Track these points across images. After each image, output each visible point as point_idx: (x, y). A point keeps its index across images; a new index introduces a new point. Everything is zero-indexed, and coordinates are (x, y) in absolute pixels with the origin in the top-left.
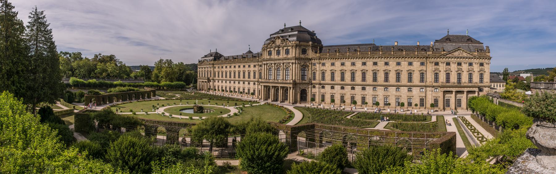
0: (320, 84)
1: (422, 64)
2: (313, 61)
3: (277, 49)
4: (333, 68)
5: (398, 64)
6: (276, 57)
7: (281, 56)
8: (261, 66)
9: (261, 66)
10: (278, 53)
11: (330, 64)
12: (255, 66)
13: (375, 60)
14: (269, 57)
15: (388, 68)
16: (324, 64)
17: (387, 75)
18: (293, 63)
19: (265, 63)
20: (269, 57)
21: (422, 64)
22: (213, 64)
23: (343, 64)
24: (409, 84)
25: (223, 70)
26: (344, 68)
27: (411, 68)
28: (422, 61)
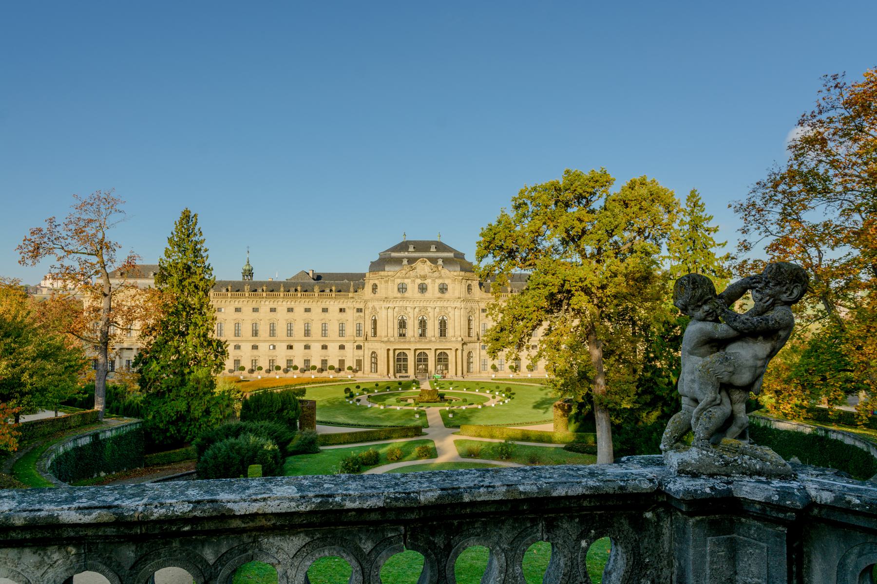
3: (419, 281)
9: (359, 310)
10: (423, 289)
20: (399, 295)
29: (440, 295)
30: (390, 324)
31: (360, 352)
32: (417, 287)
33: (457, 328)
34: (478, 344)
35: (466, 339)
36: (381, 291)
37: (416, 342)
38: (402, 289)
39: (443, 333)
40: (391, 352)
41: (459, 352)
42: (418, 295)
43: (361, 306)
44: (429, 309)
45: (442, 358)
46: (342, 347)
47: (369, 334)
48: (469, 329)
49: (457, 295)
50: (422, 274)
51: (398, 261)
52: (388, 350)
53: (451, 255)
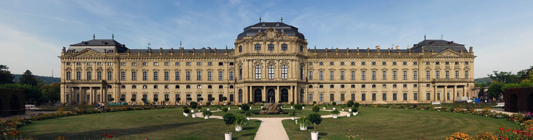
0: (319, 83)
2: (309, 60)
3: (269, 43)
4: (331, 67)
5: (395, 63)
6: (268, 52)
7: (275, 51)
8: (231, 64)
9: (231, 64)
10: (271, 47)
11: (329, 63)
12: (221, 64)
13: (374, 60)
14: (256, 52)
16: (321, 64)
18: (293, 60)
19: (250, 58)
21: (415, 63)
22: (119, 58)
23: (342, 64)
24: (404, 81)
25: (145, 68)
26: (344, 67)
29: (282, 52)
30: (250, 71)
32: (267, 46)
33: (294, 73)
35: (300, 80)
37: (267, 82)
38: (258, 47)
40: (251, 88)
41: (296, 88)
42: (268, 52)
43: (232, 61)
45: (284, 91)
46: (221, 87)
47: (238, 78)
48: (302, 74)
49: (293, 51)
52: (249, 87)
53: (290, 28)
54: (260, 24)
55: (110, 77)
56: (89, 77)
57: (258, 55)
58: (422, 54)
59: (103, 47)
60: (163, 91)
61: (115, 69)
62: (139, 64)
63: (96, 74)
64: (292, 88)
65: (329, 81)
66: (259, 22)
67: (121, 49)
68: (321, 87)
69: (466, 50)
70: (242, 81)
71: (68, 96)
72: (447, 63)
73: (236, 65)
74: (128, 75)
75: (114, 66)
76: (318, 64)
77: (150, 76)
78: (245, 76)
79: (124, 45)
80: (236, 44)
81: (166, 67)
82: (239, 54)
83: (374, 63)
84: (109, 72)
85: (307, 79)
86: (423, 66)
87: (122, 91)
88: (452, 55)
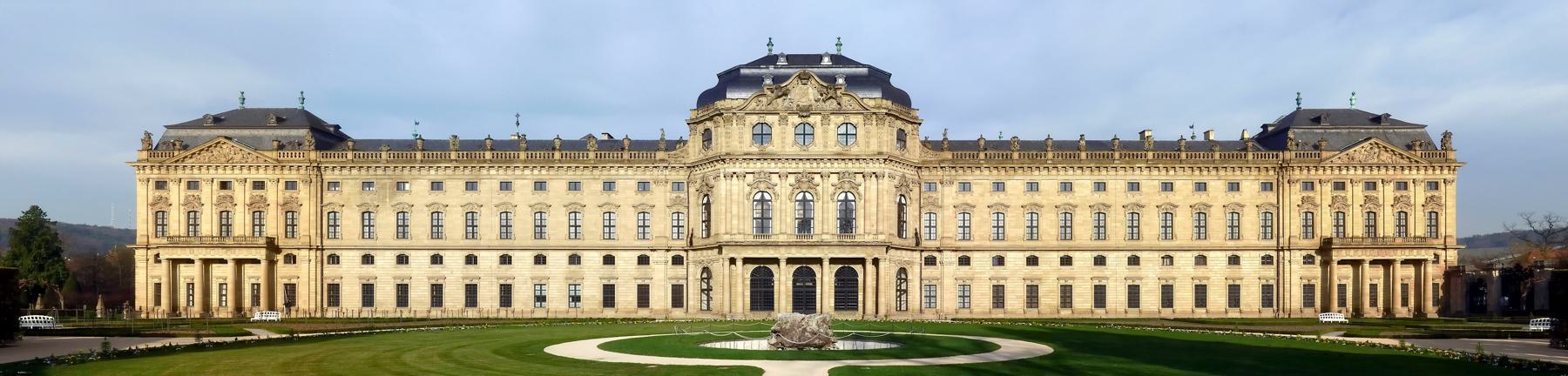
1: (1266, 187)
4: (999, 198)
5: (1201, 187)
6: (792, 150)
8: (678, 186)
9: (678, 186)
10: (805, 134)
14: (755, 149)
15: (1171, 197)
16: (965, 187)
17: (1168, 215)
19: (738, 168)
21: (1266, 187)
25: (403, 198)
26: (1037, 198)
27: (1235, 197)
28: (1263, 177)
31: (680, 271)
32: (790, 130)
34: (917, 255)
35: (897, 241)
36: (721, 144)
37: (790, 245)
38: (762, 135)
39: (847, 224)
41: (882, 265)
43: (681, 176)
44: (817, 178)
48: (901, 223)
49: (874, 148)
50: (804, 102)
51: (755, 82)
53: (865, 70)
54: (771, 60)
55: (291, 227)
56: (225, 226)
57: (764, 157)
58: (1288, 155)
59: (270, 132)
60: (459, 274)
61: (306, 204)
62: (383, 187)
63: (249, 218)
64: (870, 267)
65: (988, 244)
66: (765, 53)
67: (328, 138)
68: (965, 261)
69: (1430, 143)
70: (711, 241)
71: (158, 286)
72: (1371, 185)
73: (692, 190)
74: (350, 222)
75: (304, 193)
76: (955, 187)
77: (420, 224)
78: (721, 228)
79: (337, 127)
80: (693, 123)
81: (471, 197)
82: (701, 156)
83: (1134, 187)
84: (290, 214)
85: (917, 236)
86: (1295, 194)
87: (330, 270)
88: (1385, 157)
